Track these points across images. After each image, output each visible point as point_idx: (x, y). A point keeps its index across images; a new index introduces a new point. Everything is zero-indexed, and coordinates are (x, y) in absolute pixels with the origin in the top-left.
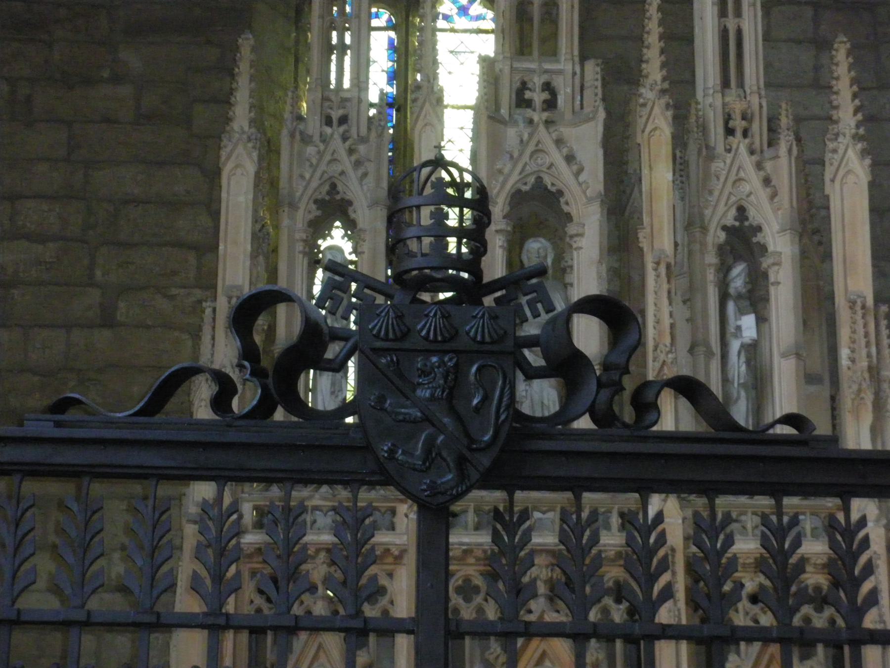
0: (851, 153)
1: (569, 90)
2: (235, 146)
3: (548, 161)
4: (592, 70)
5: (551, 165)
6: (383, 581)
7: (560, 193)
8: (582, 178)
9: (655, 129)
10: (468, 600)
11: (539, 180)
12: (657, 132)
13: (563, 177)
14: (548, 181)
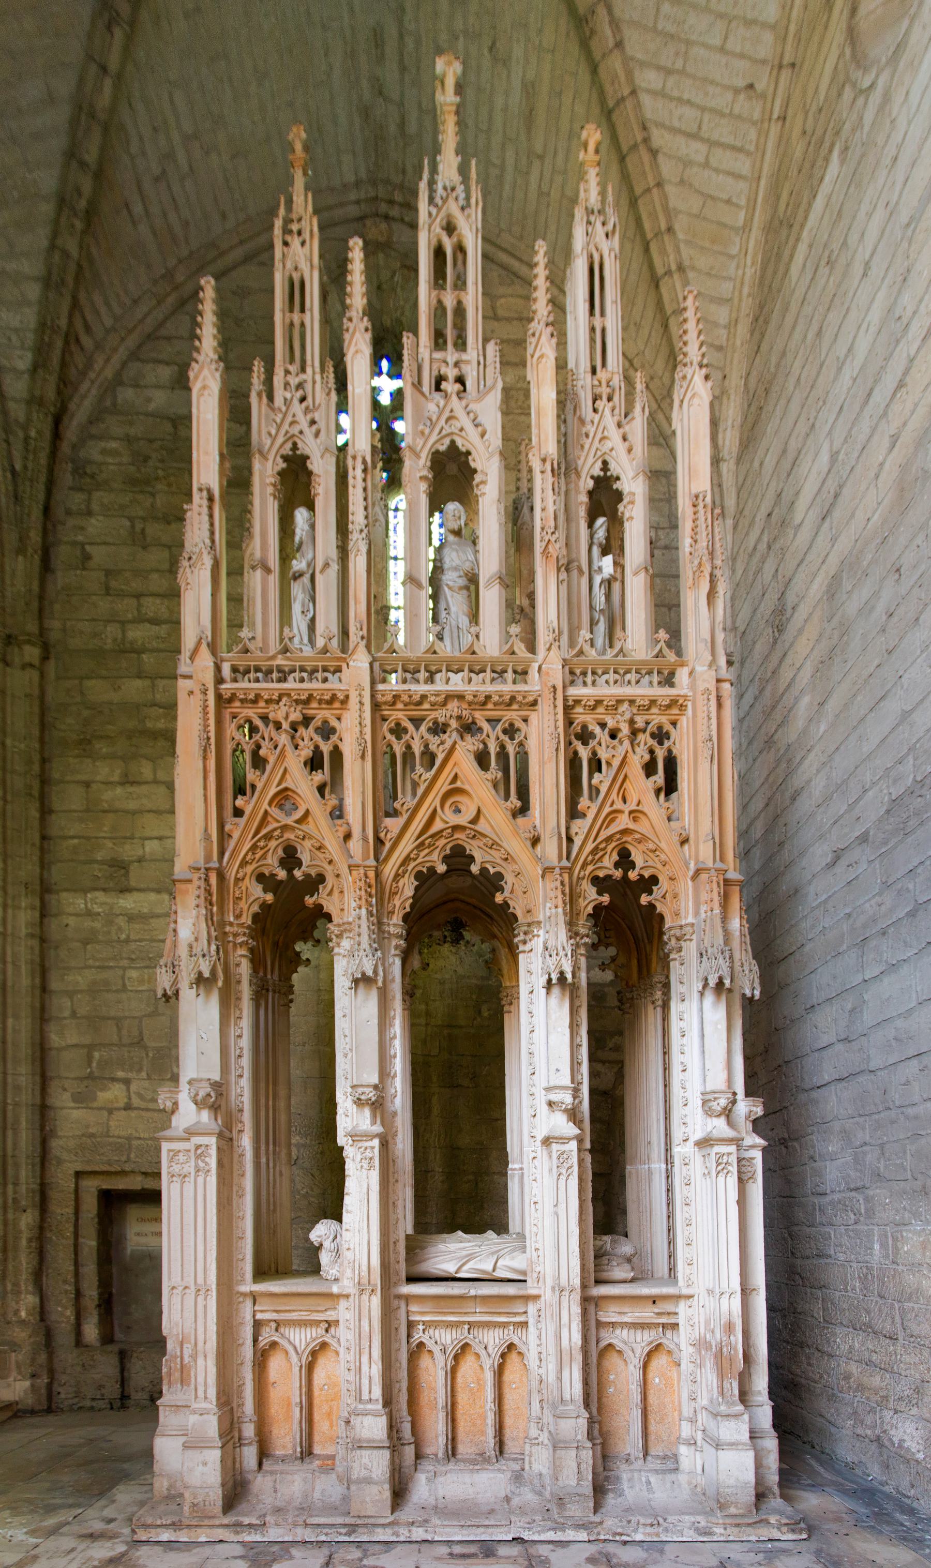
0: (696, 378)
1: (475, 373)
2: (202, 368)
3: (459, 425)
4: (491, 348)
5: (462, 430)
6: (334, 723)
7: (468, 453)
8: (486, 437)
9: (542, 356)
10: (399, 738)
11: (453, 442)
12: (544, 360)
13: (469, 440)
14: (459, 442)
